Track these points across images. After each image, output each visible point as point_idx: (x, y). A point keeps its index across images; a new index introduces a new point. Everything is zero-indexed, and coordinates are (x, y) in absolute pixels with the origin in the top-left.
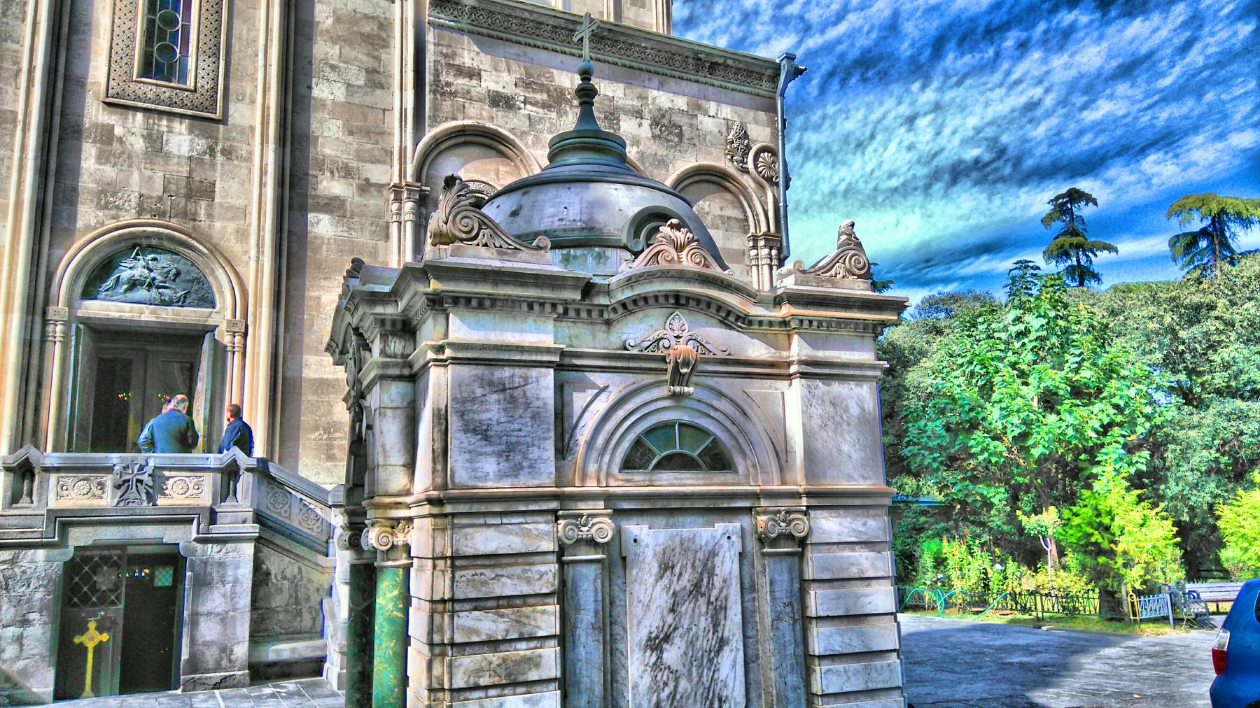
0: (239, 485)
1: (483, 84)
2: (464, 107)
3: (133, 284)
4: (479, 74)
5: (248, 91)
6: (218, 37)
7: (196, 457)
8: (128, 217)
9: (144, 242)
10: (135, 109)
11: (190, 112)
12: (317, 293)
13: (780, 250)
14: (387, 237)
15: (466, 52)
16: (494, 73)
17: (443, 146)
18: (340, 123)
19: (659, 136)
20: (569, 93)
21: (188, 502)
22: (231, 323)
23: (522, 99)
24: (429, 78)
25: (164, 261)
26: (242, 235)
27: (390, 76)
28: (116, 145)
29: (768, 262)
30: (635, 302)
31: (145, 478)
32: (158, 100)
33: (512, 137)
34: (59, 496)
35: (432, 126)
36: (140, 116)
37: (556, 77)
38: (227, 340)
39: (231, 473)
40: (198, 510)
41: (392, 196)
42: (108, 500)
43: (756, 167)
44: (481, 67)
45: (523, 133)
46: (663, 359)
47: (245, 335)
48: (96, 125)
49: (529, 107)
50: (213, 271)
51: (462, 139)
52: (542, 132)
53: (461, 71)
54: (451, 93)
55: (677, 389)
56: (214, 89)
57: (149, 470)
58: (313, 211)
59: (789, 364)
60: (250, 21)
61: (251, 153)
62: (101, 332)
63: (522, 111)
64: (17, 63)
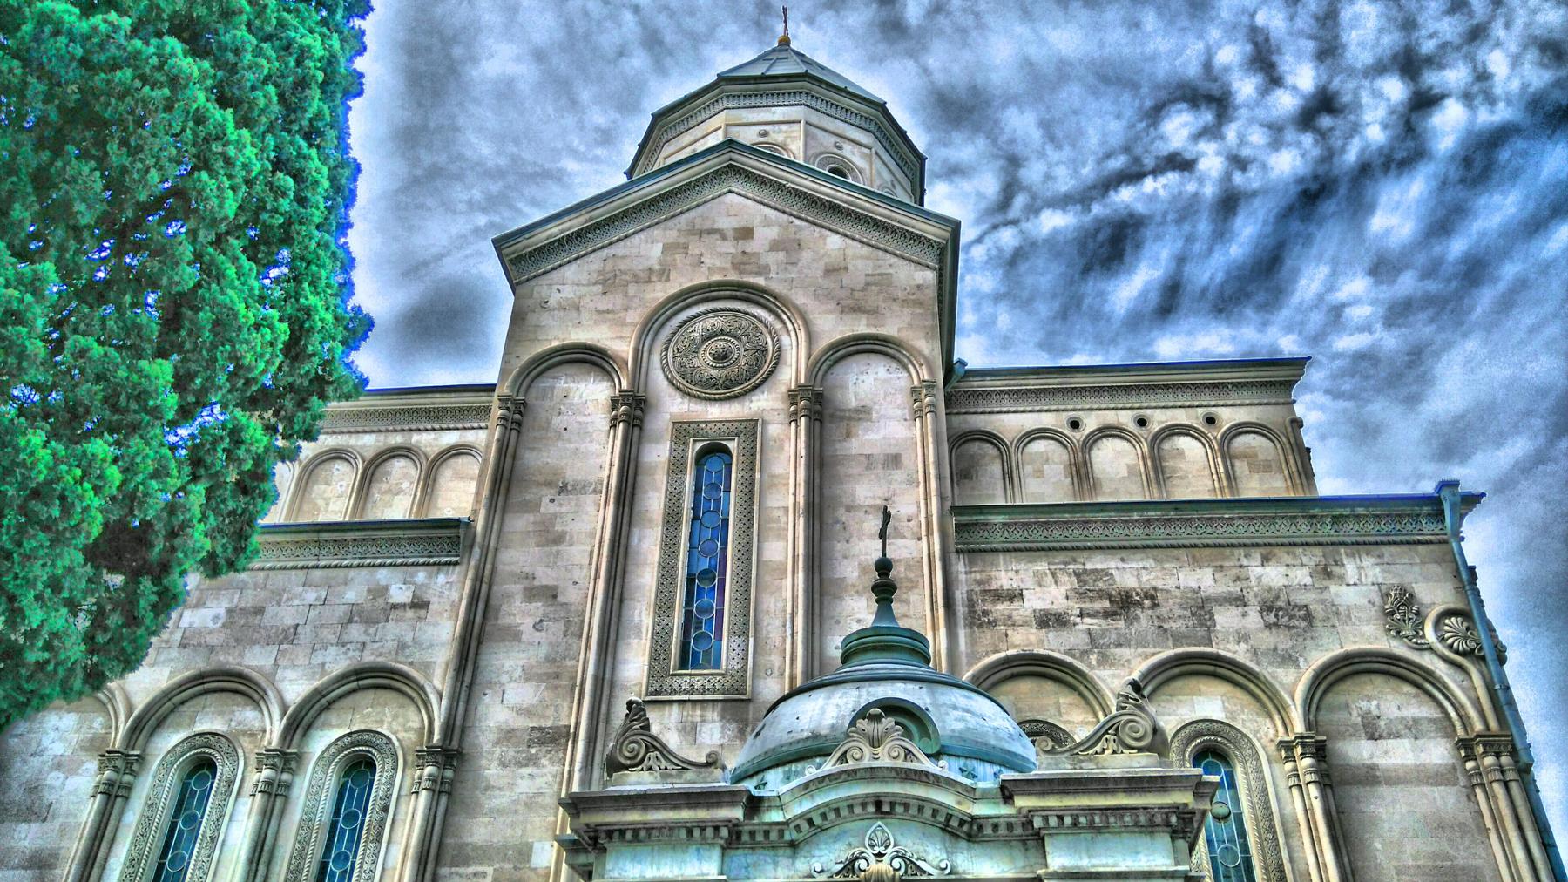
2: (1007, 635)
4: (1021, 595)
6: (747, 615)
10: (671, 702)
11: (721, 697)
13: (1514, 753)
15: (1003, 573)
16: (1038, 589)
19: (1276, 624)
20: (1137, 594)
23: (1078, 612)
29: (1498, 775)
32: (692, 691)
33: (1069, 659)
35: (970, 664)
36: (675, 707)
37: (1117, 579)
43: (1442, 640)
44: (1022, 586)
49: (1087, 620)
52: (1108, 647)
53: (999, 596)
54: (990, 622)
56: (744, 668)
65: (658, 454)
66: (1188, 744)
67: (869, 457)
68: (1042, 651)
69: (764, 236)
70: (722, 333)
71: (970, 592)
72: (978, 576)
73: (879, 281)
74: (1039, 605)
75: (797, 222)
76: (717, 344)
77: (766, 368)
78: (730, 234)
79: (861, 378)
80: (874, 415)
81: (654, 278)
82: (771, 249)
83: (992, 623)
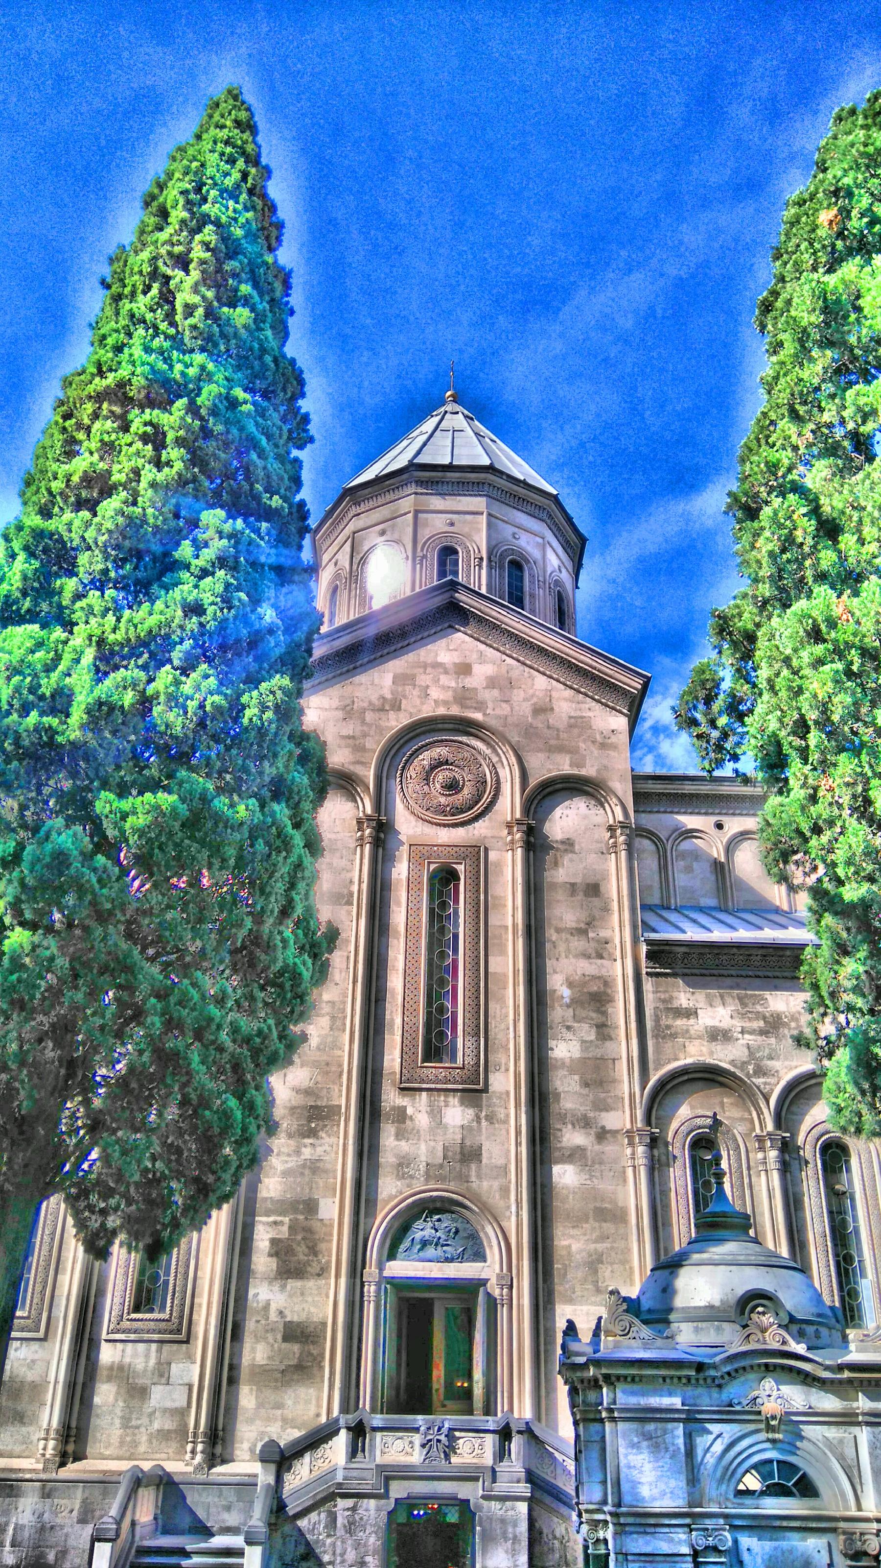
0: (513, 1446)
3: (425, 1243)
5: (503, 1061)
7: (478, 1419)
8: (418, 1186)
9: (431, 1206)
10: (421, 1090)
11: (460, 1087)
14: (625, 1181)
17: (669, 1087)
18: (577, 1077)
21: (475, 1461)
22: (500, 1277)
24: (649, 1024)
25: (447, 1221)
27: (617, 1027)
28: (408, 1122)
30: (736, 1371)
31: (442, 1438)
33: (732, 1069)
34: (383, 1453)
36: (424, 1094)
38: (496, 1293)
39: (505, 1434)
40: (480, 1468)
42: (416, 1457)
45: (744, 1063)
46: (759, 1413)
48: (393, 1108)
49: (747, 1036)
50: (483, 1228)
51: (686, 1077)
54: (671, 1035)
55: (770, 1436)
57: (444, 1430)
58: (557, 1163)
59: (857, 1415)
60: (502, 1000)
61: (508, 1116)
62: (400, 1285)
63: (741, 1042)
64: (341, 1065)
65: (400, 871)
66: (818, 1139)
67: (573, 885)
68: (712, 1062)
69: (482, 672)
70: (447, 763)
71: (656, 1008)
73: (579, 724)
74: (710, 1022)
75: (509, 661)
77: (486, 799)
79: (568, 812)
80: (577, 847)
82: (487, 687)
83: (674, 1036)
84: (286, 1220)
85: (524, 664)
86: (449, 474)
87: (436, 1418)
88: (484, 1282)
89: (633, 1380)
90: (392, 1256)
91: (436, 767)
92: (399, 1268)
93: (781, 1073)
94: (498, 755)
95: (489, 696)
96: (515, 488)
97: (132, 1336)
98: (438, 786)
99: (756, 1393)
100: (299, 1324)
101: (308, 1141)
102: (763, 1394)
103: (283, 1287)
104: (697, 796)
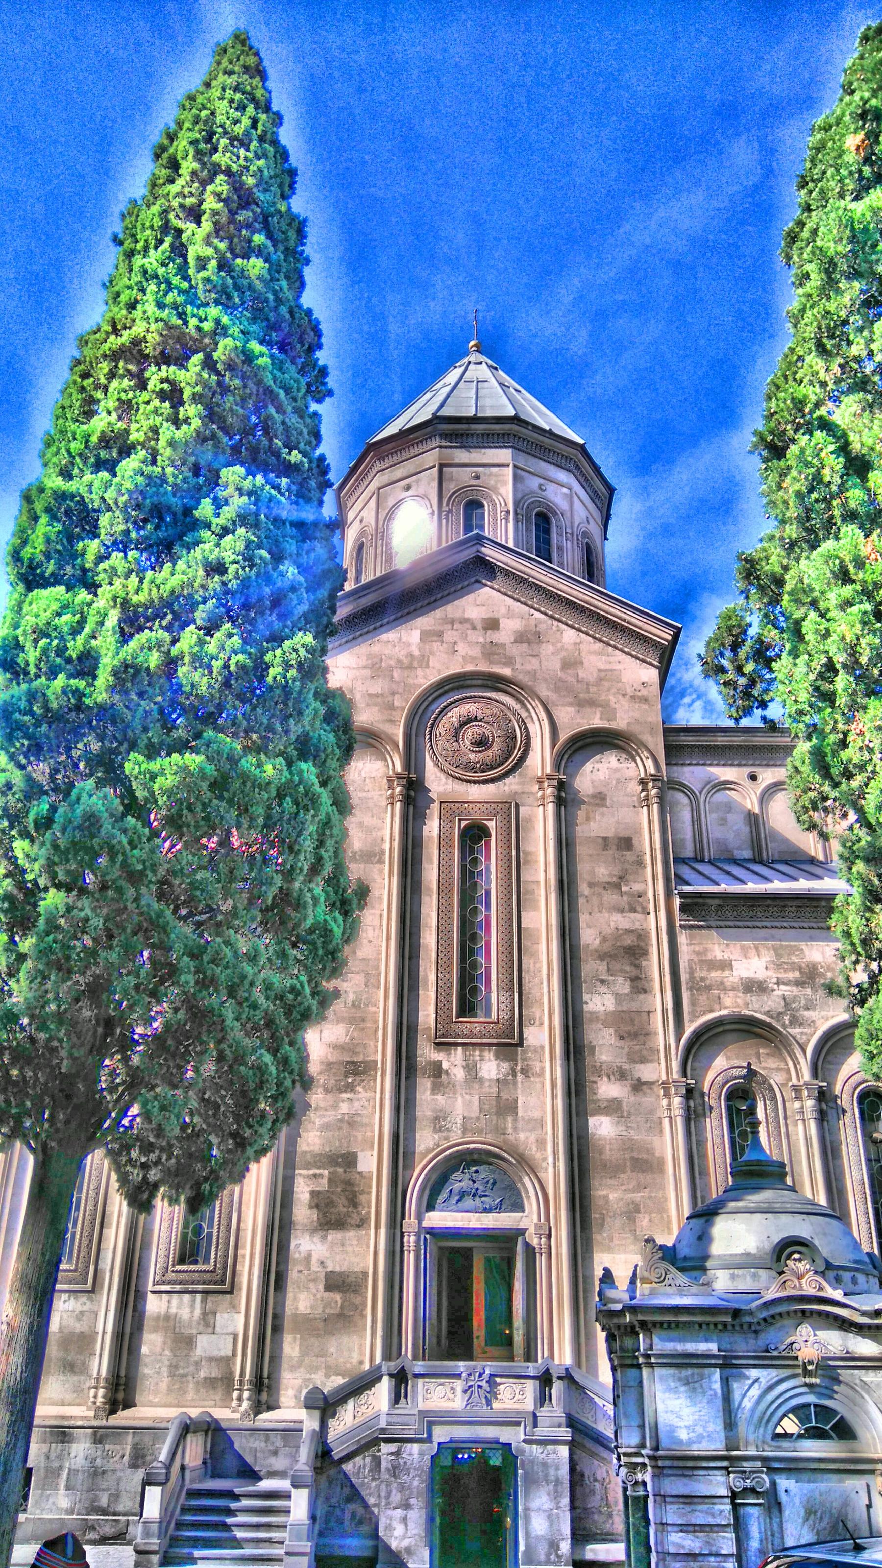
0: (553, 1391)
1: (735, 973)
3: (462, 1195)
5: (538, 1016)
7: (519, 1366)
8: (456, 1136)
9: (468, 1158)
10: (456, 1044)
11: (495, 1041)
12: (604, 1192)
14: (661, 1131)
18: (611, 1031)
22: (538, 1226)
24: (684, 977)
25: (484, 1172)
26: (541, 1143)
28: (444, 1076)
30: (773, 1317)
31: (483, 1383)
33: (768, 1020)
34: (425, 1399)
35: (691, 1021)
38: (535, 1242)
39: (545, 1379)
41: (662, 1092)
42: (458, 1403)
45: (780, 1014)
46: (796, 1358)
47: (549, 1236)
49: (782, 987)
50: (521, 1179)
55: (807, 1380)
56: (512, 1018)
57: (486, 1376)
58: (593, 1115)
60: (535, 955)
61: (543, 1069)
64: (376, 1022)
65: (432, 828)
67: (605, 839)
68: (748, 1013)
72: (697, 948)
74: (745, 974)
75: (537, 615)
76: (471, 733)
77: (517, 753)
78: (479, 626)
79: (597, 766)
80: (608, 802)
81: (415, 664)
82: (516, 641)
84: (326, 1172)
85: (552, 617)
86: (473, 426)
87: (478, 1364)
88: (522, 1232)
89: (669, 1327)
90: (431, 1207)
91: (465, 724)
92: (438, 1219)
93: (818, 1023)
94: (528, 710)
95: (515, 651)
96: (541, 438)
97: (178, 1288)
98: (468, 743)
99: (792, 1339)
100: (340, 1274)
101: (345, 1096)
102: (800, 1340)
103: (324, 1238)
104: (730, 747)
